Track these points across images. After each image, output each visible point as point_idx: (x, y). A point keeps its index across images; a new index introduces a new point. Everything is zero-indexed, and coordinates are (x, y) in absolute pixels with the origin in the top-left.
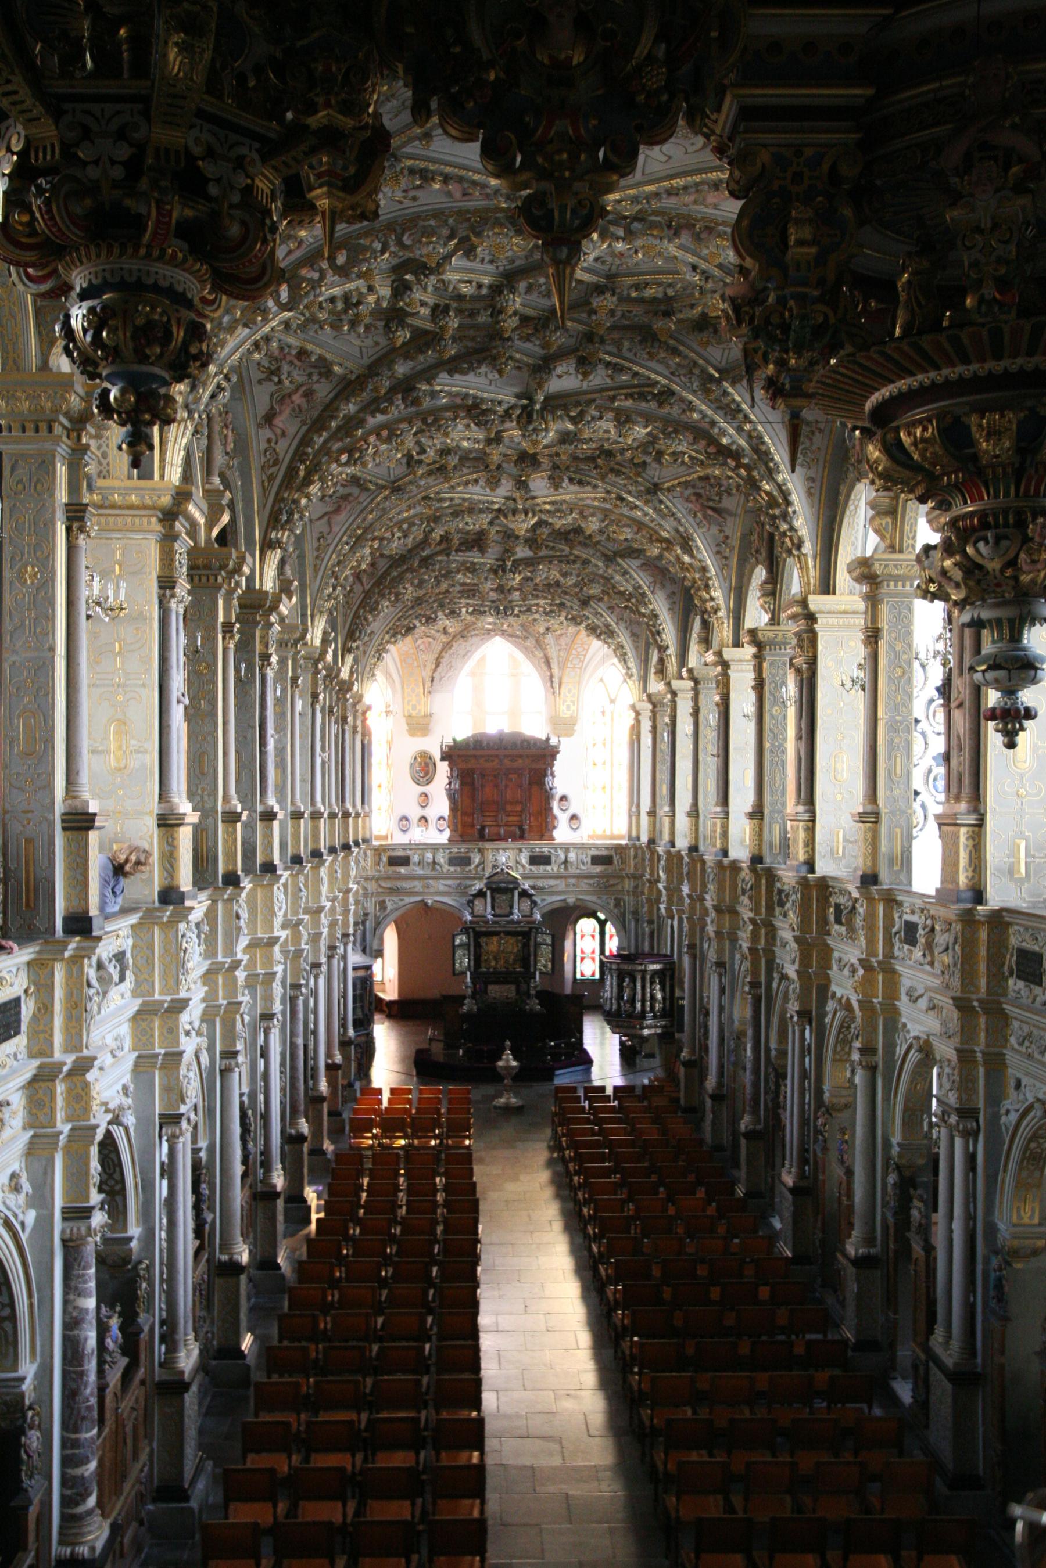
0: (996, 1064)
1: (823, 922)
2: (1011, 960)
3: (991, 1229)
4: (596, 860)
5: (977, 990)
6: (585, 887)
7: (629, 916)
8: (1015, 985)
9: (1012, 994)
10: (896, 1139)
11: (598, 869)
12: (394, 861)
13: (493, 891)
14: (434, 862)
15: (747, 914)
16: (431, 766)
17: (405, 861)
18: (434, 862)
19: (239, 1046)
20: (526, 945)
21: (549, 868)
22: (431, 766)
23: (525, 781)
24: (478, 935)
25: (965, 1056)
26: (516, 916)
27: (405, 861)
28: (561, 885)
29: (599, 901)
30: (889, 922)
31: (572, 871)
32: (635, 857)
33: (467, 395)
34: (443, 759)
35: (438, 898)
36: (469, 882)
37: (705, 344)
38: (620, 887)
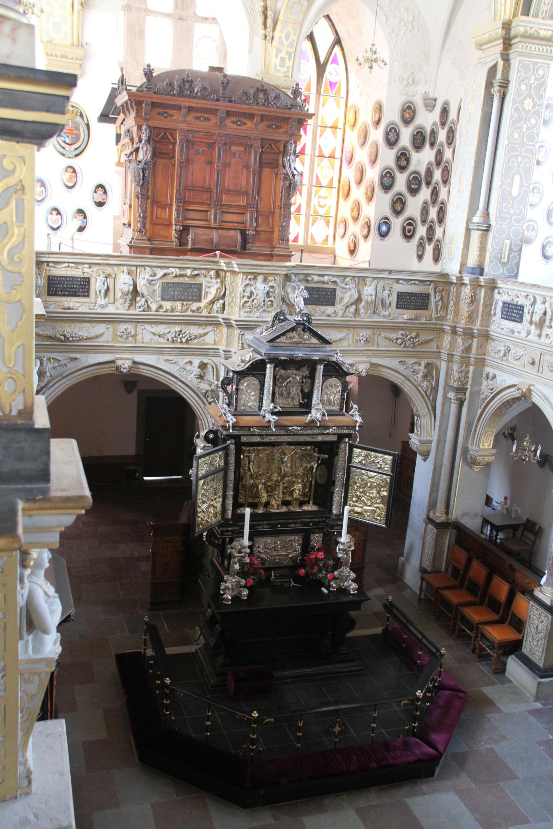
4: (406, 301)
6: (384, 345)
11: (406, 315)
12: (56, 287)
13: (278, 363)
14: (135, 292)
16: (83, 129)
17: (80, 287)
18: (135, 292)
20: (329, 465)
21: (330, 310)
22: (83, 129)
23: (253, 159)
24: (239, 445)
26: (315, 414)
27: (80, 287)
29: (401, 368)
31: (365, 316)
32: (473, 300)
34: (105, 117)
35: (139, 358)
36: (195, 330)
38: (433, 347)
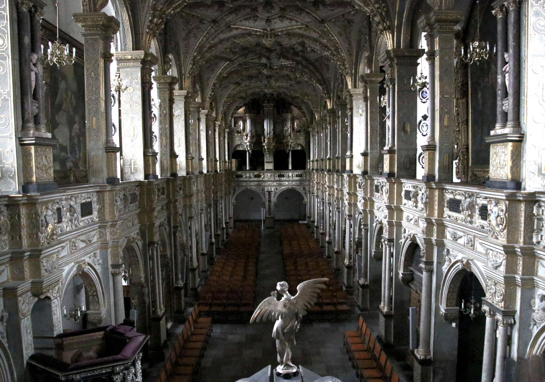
0: (399, 225)
1: (356, 188)
2: (403, 194)
3: (397, 274)
5: (394, 204)
7: (307, 192)
8: (404, 201)
9: (403, 203)
10: (373, 250)
11: (298, 178)
15: (335, 186)
19: (178, 225)
25: (390, 223)
28: (287, 183)
30: (372, 185)
33: (247, 29)
37: (316, 10)
